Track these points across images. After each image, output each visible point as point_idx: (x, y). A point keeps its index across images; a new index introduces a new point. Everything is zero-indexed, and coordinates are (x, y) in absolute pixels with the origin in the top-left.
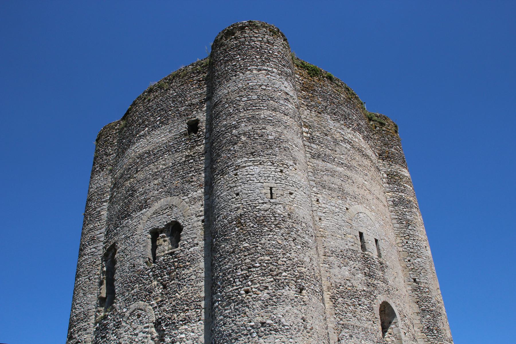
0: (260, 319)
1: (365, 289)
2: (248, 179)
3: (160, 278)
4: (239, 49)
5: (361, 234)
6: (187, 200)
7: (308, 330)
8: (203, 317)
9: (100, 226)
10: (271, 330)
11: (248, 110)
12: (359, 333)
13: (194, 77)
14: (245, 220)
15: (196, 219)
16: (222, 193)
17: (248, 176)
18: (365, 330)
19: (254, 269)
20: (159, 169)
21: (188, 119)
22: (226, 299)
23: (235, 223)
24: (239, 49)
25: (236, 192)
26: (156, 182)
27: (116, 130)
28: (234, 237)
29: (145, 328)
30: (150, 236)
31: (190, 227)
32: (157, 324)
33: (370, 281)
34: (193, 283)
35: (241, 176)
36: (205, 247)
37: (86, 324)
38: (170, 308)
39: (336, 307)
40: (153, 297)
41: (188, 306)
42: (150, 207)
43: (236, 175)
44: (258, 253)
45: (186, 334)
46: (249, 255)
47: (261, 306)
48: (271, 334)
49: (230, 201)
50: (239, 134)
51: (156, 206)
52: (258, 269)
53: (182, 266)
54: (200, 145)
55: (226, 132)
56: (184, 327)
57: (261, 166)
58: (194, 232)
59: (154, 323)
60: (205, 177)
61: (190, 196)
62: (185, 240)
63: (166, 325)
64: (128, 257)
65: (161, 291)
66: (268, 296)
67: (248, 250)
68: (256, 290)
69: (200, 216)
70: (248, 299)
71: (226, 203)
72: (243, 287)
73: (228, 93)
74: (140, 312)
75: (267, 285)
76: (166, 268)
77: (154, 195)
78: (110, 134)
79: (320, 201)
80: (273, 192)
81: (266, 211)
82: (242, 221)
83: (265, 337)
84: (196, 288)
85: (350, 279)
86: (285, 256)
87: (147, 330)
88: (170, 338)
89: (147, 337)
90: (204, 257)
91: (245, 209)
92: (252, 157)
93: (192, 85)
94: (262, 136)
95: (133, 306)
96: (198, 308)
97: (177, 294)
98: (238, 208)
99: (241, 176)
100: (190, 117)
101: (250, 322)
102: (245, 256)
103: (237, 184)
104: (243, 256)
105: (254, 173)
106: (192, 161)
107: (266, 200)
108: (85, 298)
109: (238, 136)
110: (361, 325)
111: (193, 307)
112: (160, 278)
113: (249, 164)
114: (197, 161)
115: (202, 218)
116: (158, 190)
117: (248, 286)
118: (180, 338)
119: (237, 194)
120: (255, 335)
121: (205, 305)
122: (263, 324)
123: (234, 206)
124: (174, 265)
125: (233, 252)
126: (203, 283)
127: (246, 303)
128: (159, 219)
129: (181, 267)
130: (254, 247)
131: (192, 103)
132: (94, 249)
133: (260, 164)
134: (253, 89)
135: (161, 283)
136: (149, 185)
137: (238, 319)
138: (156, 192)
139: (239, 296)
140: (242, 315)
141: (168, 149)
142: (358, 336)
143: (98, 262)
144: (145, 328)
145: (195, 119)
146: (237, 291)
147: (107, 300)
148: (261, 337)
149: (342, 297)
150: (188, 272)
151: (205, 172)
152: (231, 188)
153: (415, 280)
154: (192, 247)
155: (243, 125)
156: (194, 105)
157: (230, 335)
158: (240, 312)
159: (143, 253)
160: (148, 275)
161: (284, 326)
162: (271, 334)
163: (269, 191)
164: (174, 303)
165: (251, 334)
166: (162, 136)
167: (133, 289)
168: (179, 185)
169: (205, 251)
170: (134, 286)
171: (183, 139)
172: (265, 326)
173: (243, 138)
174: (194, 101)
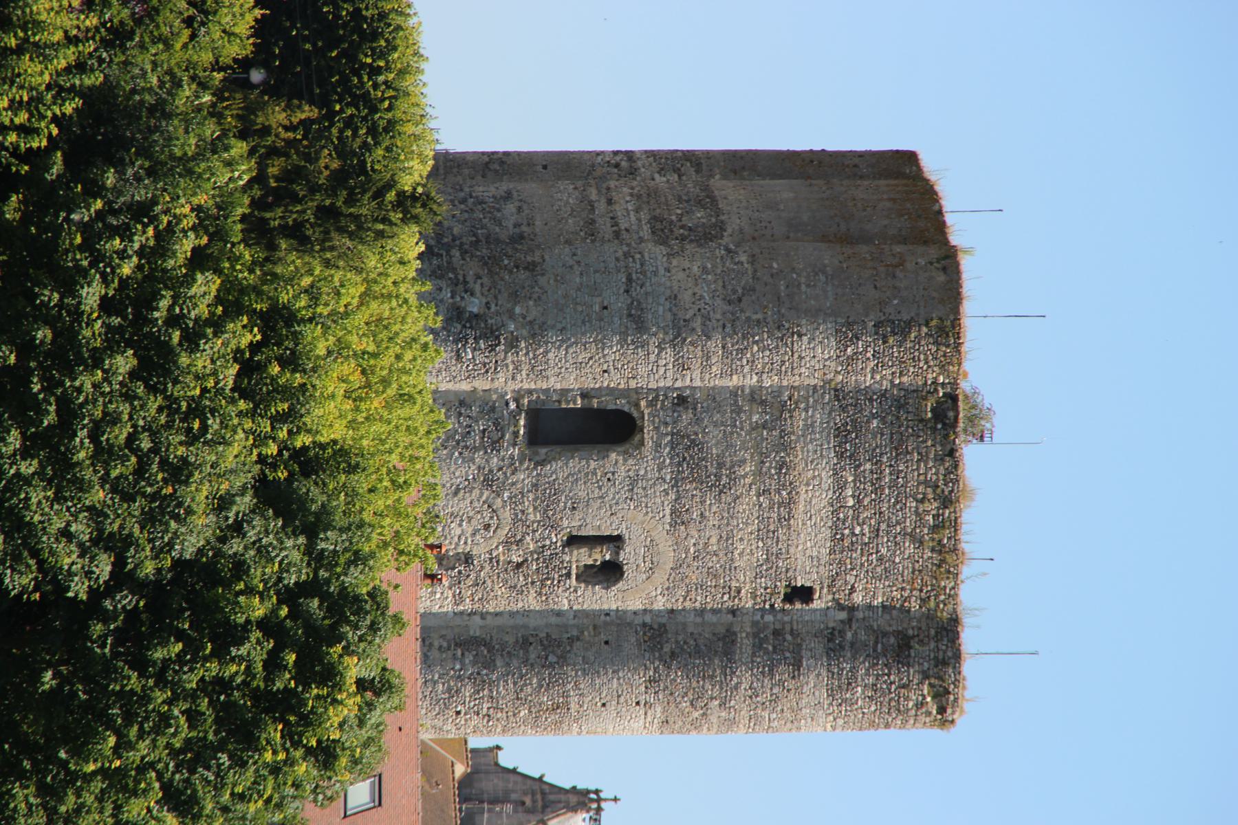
26: (714, 540)
32: (468, 559)
37: (524, 376)
61: (660, 597)
63: (460, 572)
76: (547, 567)
119: (604, 705)
124: (548, 579)
135: (526, 560)
138: (693, 541)
152: (619, 696)
167: (535, 508)
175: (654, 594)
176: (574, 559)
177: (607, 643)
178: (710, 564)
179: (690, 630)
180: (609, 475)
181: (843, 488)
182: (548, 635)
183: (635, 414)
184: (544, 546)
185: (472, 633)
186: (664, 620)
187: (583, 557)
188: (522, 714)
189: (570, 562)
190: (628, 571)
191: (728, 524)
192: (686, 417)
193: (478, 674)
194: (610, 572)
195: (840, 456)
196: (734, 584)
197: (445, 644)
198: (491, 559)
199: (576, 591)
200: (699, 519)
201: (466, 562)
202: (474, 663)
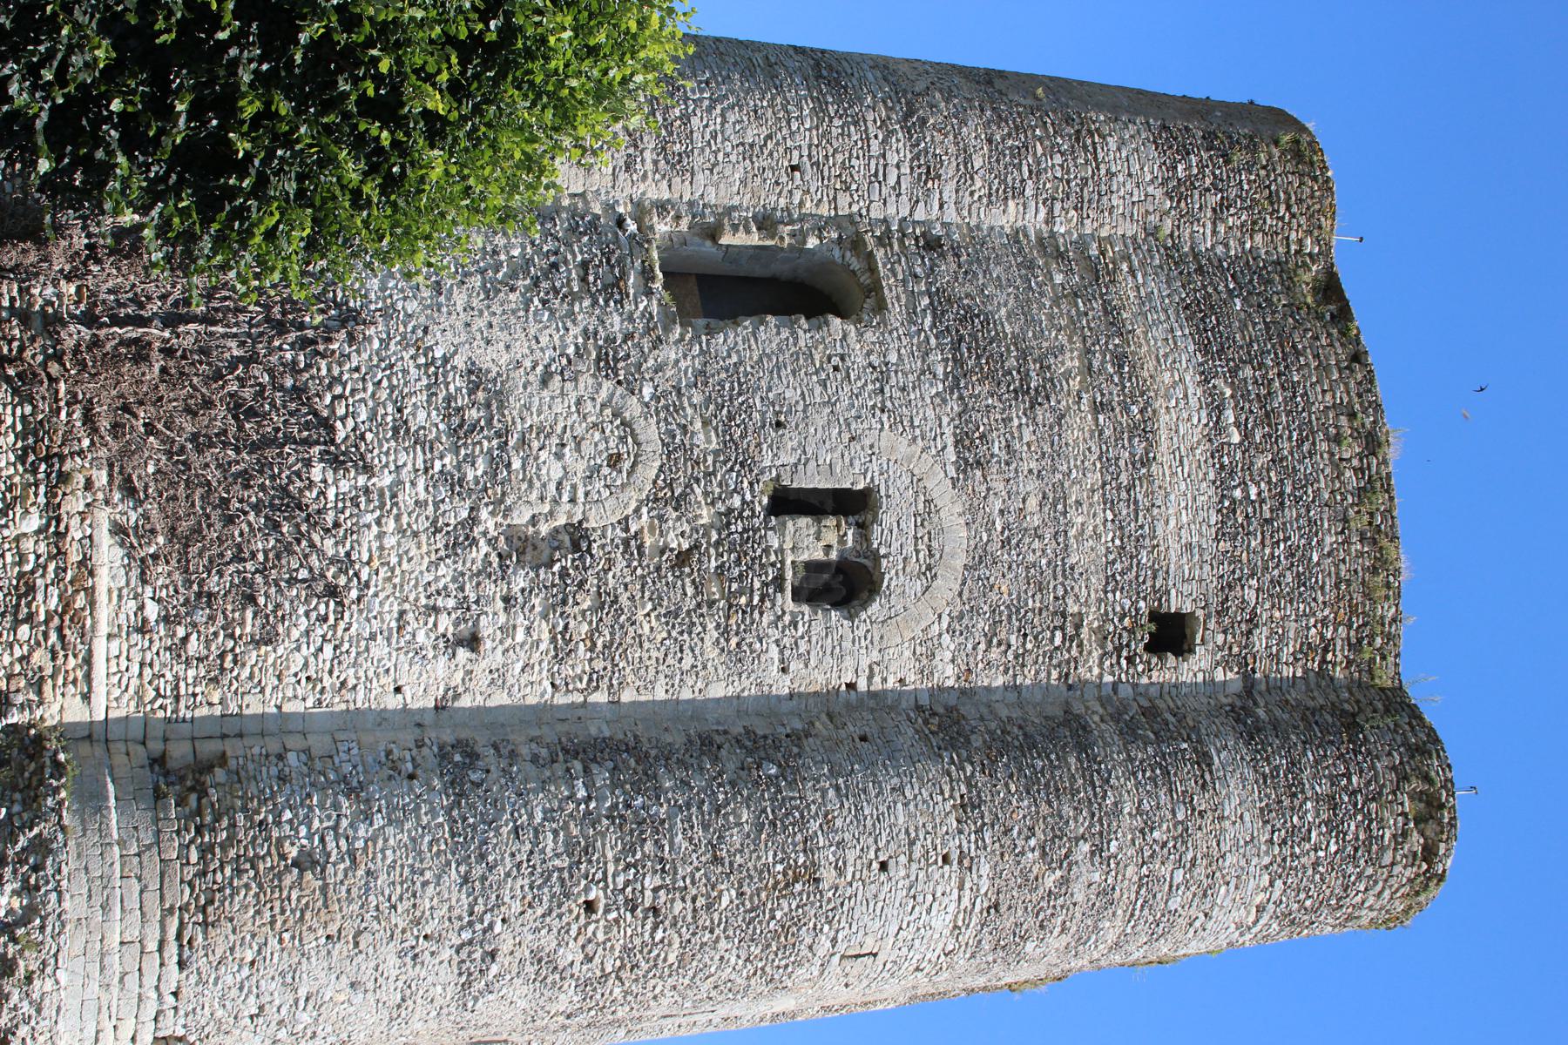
0: (505, 948)
2: (920, 899)
3: (714, 537)
4: (1356, 850)
6: (936, 629)
8: (561, 699)
9: (967, 199)
10: (470, 974)
11: (1140, 887)
13: (1350, 627)
14: (800, 894)
15: (865, 663)
16: (905, 805)
17: (929, 897)
19: (648, 927)
20: (1072, 512)
21: (1208, 616)
22: (586, 838)
23: (801, 861)
24: (1356, 850)
25: (892, 863)
26: (1033, 503)
27: (1300, 242)
28: (759, 858)
29: (574, 487)
30: (860, 486)
31: (847, 644)
32: (577, 538)
34: (670, 661)
35: (937, 876)
36: (769, 697)
37: (649, 166)
38: (611, 582)
40: (661, 518)
41: (605, 646)
42: (954, 481)
43: (946, 859)
44: (694, 934)
45: (522, 645)
46: (695, 910)
48: (460, 974)
49: (871, 840)
50: (1070, 865)
51: (951, 511)
52: (647, 935)
53: (732, 621)
54: (1101, 664)
55: (1093, 815)
56: (546, 636)
57: (946, 932)
58: (828, 658)
59: (580, 523)
60: (988, 689)
61: (946, 638)
62: (808, 631)
63: (564, 574)
64: (818, 390)
65: (674, 545)
66: (561, 964)
67: (709, 907)
68: (590, 934)
69: (870, 677)
70: (571, 911)
71: (869, 822)
72: (606, 897)
73: (1222, 818)
74: (627, 465)
75: (597, 960)
76: (738, 562)
77: (992, 497)
78: (1293, 216)
81: (810, 948)
82: (798, 887)
83: (456, 959)
84: (652, 671)
87: (565, 498)
88: (523, 590)
89: (542, 499)
90: (738, 697)
91: (830, 894)
92: (986, 905)
93: (1324, 622)
94: (1042, 927)
95: (650, 433)
96: (590, 680)
97: (649, 606)
98: (841, 872)
99: (937, 876)
100: (1212, 625)
101: (503, 920)
102: (694, 900)
103: (914, 866)
104: (694, 892)
105: (934, 913)
106: (1058, 641)
107: (841, 947)
108: (733, 158)
109: (1067, 860)
111: (599, 665)
112: (714, 537)
113: (966, 902)
114: (1051, 658)
115: (862, 685)
116: (1002, 512)
117: (607, 911)
118: (514, 627)
119: (884, 866)
120: (466, 935)
121: (596, 704)
122: (493, 955)
123: (851, 855)
124: (741, 592)
125: (717, 860)
126: (660, 695)
127: (559, 907)
128: (903, 525)
129: (728, 617)
130: (712, 922)
131: (1257, 626)
132: (892, 180)
133: (956, 927)
134: (1205, 895)
135: (696, 546)
136: (1030, 471)
137: (520, 882)
138: (998, 505)
139: (583, 882)
140: (529, 897)
141: (1132, 543)
143: (843, 200)
144: (574, 487)
145: (1198, 641)
146: (599, 876)
147: (708, 243)
148: (458, 952)
150: (708, 643)
151: (1005, 687)
152: (912, 843)
154: (781, 652)
155: (1096, 877)
156: (1250, 632)
157: (482, 857)
158: (539, 888)
159: (812, 464)
160: (735, 490)
161: (476, 999)
162: (460, 974)
164: (624, 599)
165: (471, 924)
166: (1183, 514)
167: (706, 423)
168: (993, 596)
169: (756, 698)
170: (716, 429)
171: (1142, 604)
172: (483, 960)
173: (1050, 881)
174: (1260, 640)
175: (936, 629)
176: (788, 545)
177: (863, 739)
178: (1031, 558)
179: (1004, 713)
180: (836, 361)
181: (1220, 409)
182: (748, 731)
183: (855, 264)
184: (730, 511)
185: (593, 731)
186: (952, 702)
187: (810, 542)
188: (725, 901)
189: (781, 550)
190: (892, 577)
191: (1054, 470)
192: (946, 268)
193: (628, 806)
194: (845, 586)
195: (1205, 349)
196: (1073, 608)
197: (544, 752)
198: (626, 542)
199: (794, 624)
200: (1004, 456)
201: (576, 547)
202: (615, 784)
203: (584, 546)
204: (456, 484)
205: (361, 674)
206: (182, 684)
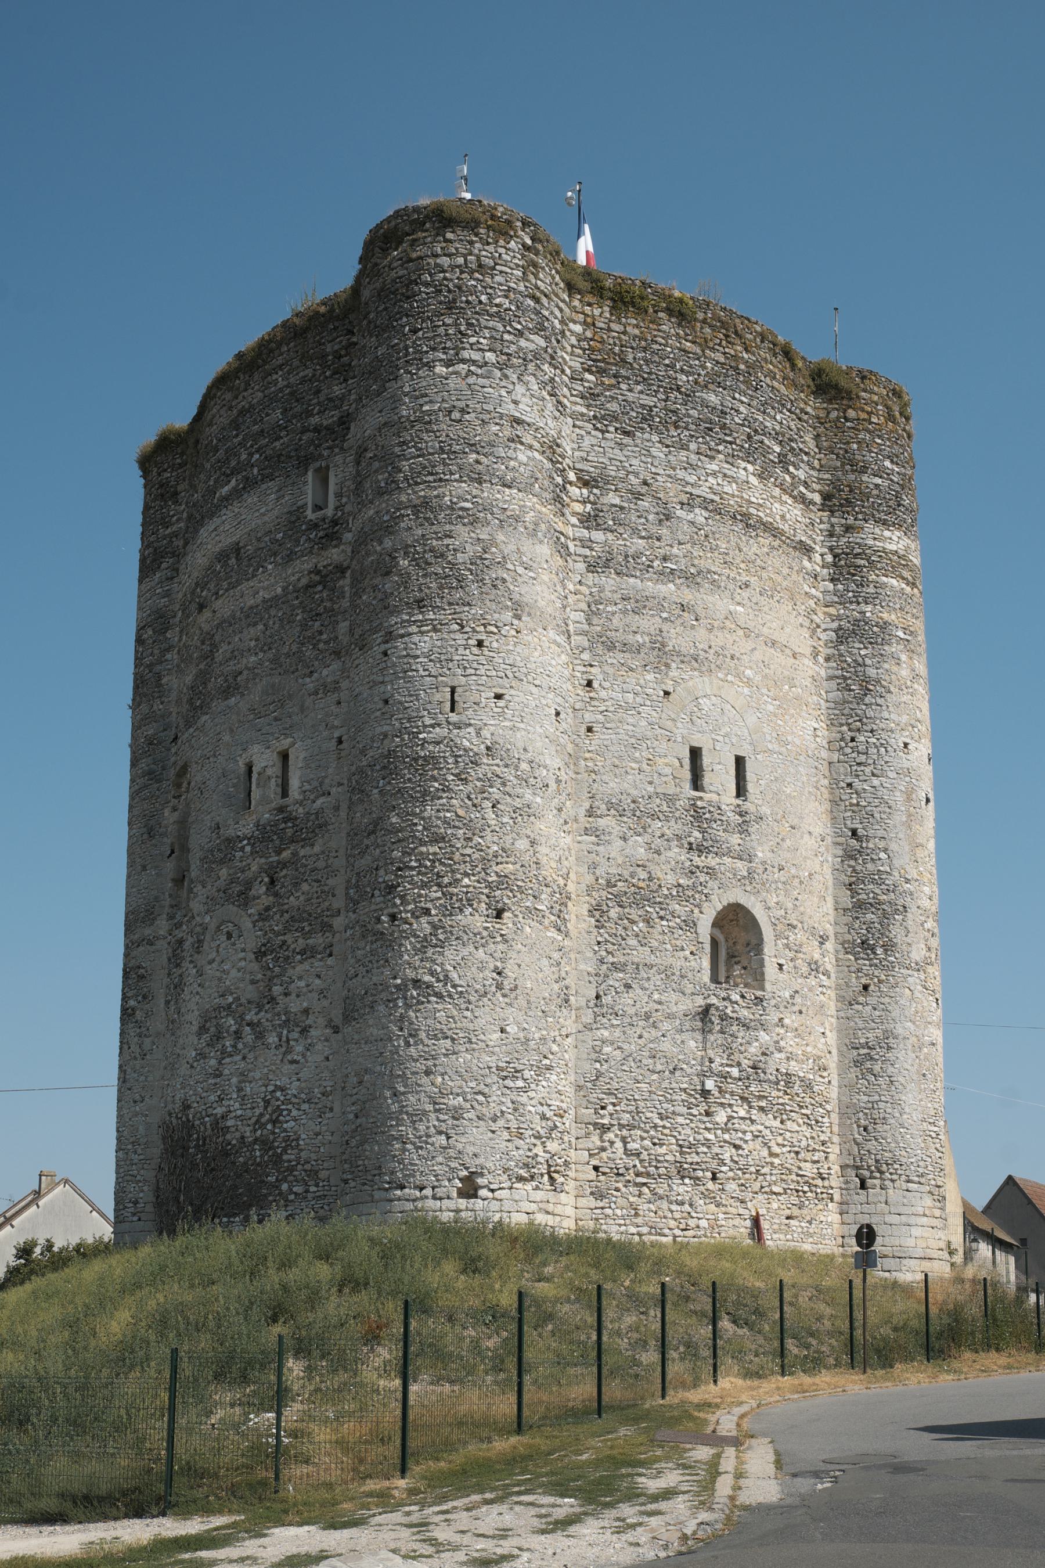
1: (681, 881)
5: (695, 754)
7: (506, 991)
10: (429, 995)
12: (649, 979)
18: (667, 972)
33: (697, 861)
39: (603, 927)
47: (414, 948)
72: (387, 907)
75: (429, 905)
79: (595, 684)
80: (456, 698)
81: (438, 743)
85: (647, 863)
86: (470, 844)
110: (658, 961)
142: (646, 985)
149: (621, 906)
153: (854, 832)
161: (454, 986)
162: (429, 1002)
163: (448, 696)
172: (420, 987)
203: (263, 949)
204: (238, 1035)
205: (317, 1084)
206: (318, 1194)
